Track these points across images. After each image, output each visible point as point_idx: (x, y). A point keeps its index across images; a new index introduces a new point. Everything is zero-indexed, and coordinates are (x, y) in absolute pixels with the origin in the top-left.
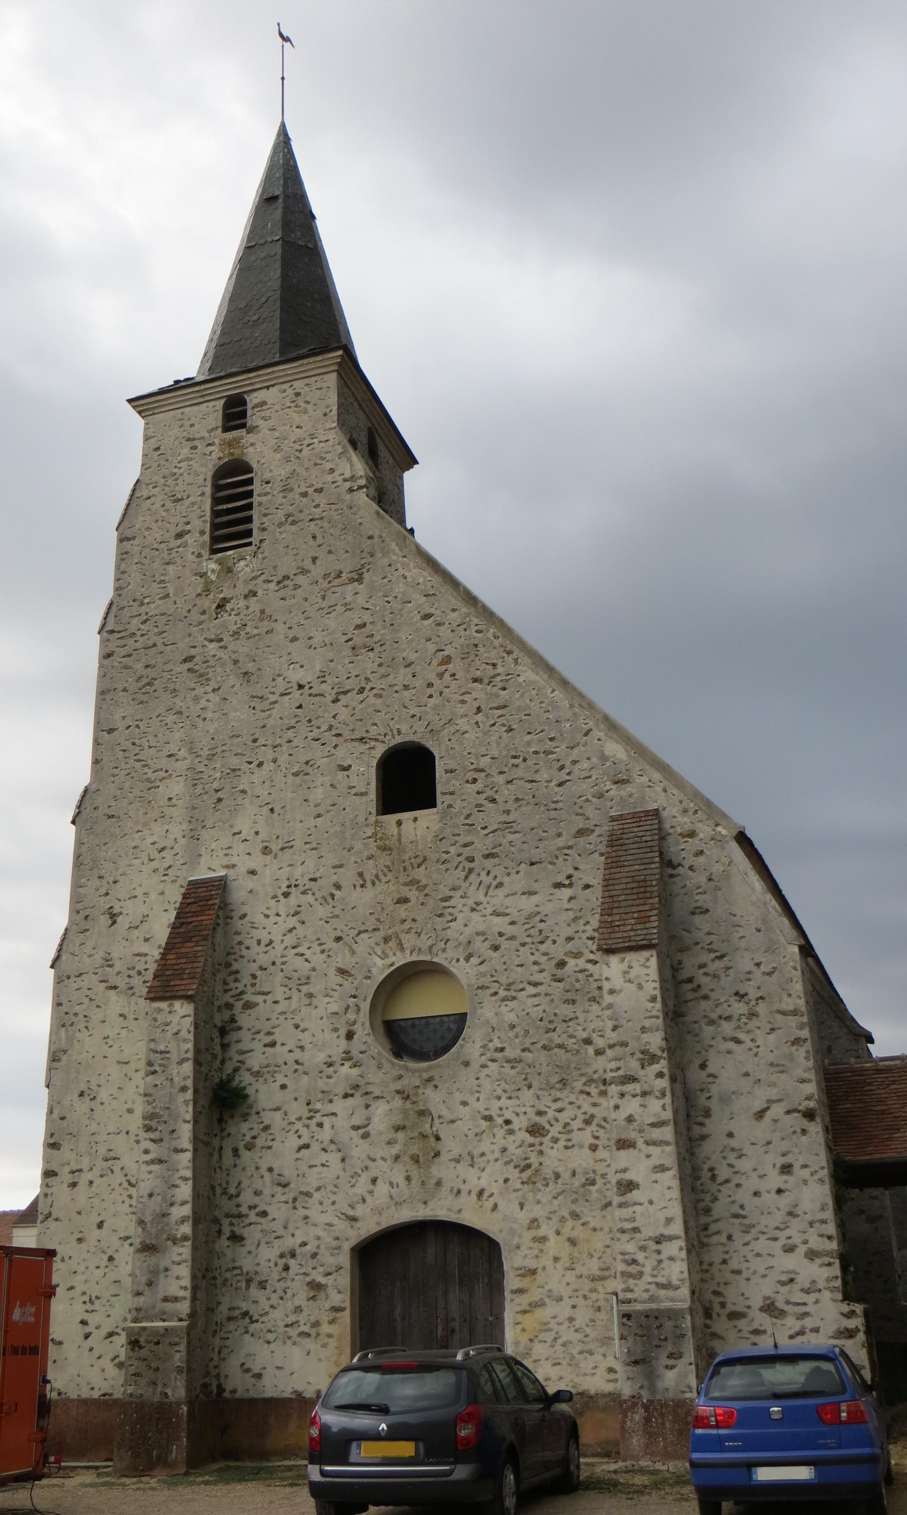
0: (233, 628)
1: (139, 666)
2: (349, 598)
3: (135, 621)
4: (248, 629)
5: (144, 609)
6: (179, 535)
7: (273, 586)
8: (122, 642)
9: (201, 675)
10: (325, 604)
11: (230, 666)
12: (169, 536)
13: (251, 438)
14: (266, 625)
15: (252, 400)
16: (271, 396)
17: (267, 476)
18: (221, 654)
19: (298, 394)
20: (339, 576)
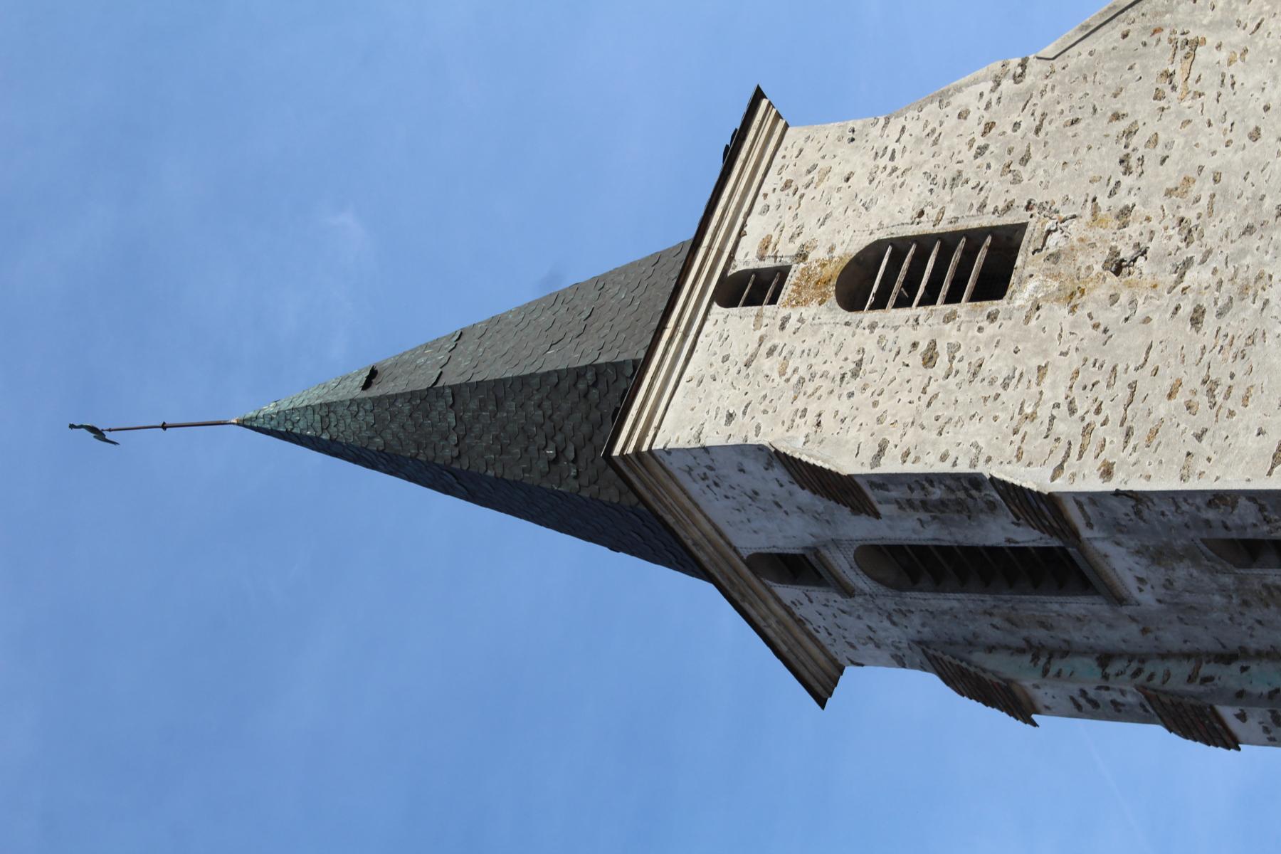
0: (1177, 240)
1: (1163, 409)
2: (1223, 55)
3: (1060, 428)
4: (1191, 215)
5: (1044, 413)
6: (929, 359)
7: (1127, 181)
8: (1092, 449)
9: (1244, 289)
10: (1211, 94)
11: (1254, 241)
12: (918, 374)
13: (816, 255)
14: (1204, 188)
15: (747, 259)
16: (758, 227)
17: (910, 214)
18: (1216, 261)
19: (787, 185)
20: (1169, 76)
